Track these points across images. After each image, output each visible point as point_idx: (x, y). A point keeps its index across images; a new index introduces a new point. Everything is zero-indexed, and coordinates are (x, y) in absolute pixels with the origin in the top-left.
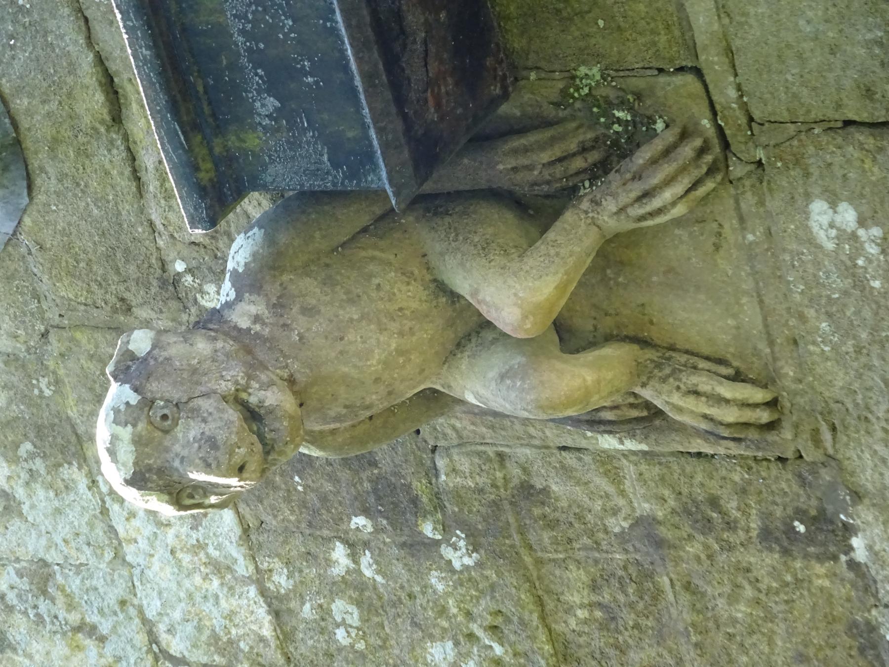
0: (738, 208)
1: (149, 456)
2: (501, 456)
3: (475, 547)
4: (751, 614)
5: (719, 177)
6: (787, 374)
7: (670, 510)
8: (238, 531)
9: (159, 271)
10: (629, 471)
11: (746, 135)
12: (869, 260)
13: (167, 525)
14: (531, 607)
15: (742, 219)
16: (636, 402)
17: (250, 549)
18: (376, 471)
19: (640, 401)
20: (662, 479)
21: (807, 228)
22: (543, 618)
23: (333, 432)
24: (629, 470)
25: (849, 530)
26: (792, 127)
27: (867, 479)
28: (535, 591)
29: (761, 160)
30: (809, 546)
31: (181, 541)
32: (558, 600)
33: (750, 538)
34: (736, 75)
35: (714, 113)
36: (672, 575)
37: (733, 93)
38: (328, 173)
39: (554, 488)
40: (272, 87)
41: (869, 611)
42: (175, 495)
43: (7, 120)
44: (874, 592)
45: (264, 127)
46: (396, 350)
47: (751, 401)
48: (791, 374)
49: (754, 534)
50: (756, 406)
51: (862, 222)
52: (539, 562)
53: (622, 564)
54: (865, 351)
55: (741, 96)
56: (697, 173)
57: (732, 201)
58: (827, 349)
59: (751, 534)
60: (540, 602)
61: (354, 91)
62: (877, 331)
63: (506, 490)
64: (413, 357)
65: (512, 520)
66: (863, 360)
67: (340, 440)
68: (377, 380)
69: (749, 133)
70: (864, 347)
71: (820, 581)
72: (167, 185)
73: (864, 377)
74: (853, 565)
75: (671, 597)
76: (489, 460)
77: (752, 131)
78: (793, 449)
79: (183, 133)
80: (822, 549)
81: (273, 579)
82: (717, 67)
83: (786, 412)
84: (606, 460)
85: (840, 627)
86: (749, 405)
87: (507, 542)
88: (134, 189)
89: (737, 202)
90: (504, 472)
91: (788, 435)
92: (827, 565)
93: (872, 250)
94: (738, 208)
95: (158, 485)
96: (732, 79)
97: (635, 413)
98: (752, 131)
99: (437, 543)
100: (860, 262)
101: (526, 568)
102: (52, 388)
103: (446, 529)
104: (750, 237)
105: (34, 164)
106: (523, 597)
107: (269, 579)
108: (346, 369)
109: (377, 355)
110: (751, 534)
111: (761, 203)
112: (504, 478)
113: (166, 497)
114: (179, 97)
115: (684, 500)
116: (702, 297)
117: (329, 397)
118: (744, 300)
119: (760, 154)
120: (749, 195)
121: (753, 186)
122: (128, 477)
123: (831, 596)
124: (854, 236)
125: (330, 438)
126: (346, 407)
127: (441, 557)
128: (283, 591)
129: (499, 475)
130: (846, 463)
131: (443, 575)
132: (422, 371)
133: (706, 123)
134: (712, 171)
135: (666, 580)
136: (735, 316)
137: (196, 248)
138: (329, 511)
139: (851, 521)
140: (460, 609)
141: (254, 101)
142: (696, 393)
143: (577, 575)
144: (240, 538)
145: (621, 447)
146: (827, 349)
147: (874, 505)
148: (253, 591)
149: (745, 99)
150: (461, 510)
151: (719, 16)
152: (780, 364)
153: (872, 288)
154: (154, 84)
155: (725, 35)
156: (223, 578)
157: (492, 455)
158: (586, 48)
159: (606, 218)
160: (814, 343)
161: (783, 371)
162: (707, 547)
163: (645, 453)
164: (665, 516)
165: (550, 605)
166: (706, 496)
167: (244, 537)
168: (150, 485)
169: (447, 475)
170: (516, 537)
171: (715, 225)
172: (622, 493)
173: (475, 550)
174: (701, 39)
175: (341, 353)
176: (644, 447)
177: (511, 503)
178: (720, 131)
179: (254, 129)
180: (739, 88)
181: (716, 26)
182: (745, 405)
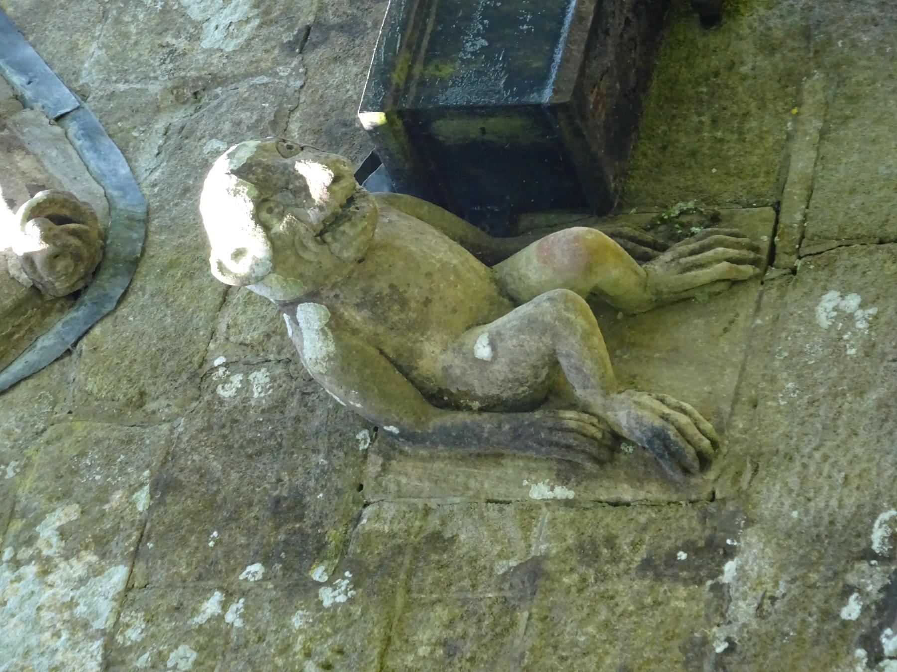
0: (759, 302)
1: (264, 157)
2: (427, 511)
3: (356, 584)
4: (594, 637)
5: (758, 271)
6: (737, 426)
7: (565, 547)
8: (121, 587)
9: (196, 366)
10: (544, 518)
11: (794, 247)
12: (854, 334)
13: (50, 586)
14: (378, 643)
15: (758, 309)
16: (598, 425)
17: (120, 606)
18: (297, 525)
19: (601, 426)
20: (572, 522)
21: (812, 311)
22: (382, 655)
23: (355, 331)
24: (546, 515)
25: (729, 553)
26: (835, 243)
27: (766, 509)
28: (388, 631)
29: (796, 267)
30: (682, 571)
31: (54, 599)
32: (407, 641)
33: (630, 569)
34: (807, 207)
35: (775, 234)
36: (534, 610)
37: (799, 217)
38: (498, 92)
39: (463, 537)
40: (487, 34)
41: (711, 627)
42: (262, 197)
43: (140, 245)
44: (723, 610)
45: (463, 61)
46: (455, 266)
47: (701, 426)
48: (741, 425)
49: (634, 566)
50: (704, 433)
51: (862, 306)
52: (408, 606)
53: (489, 602)
54: (816, 404)
55: (804, 221)
56: (745, 253)
57: (757, 295)
58: (782, 403)
59: (631, 566)
60: (388, 640)
61: (557, 36)
62: (835, 387)
63: (415, 537)
64: (459, 286)
65: (407, 562)
66: (812, 410)
67: (355, 342)
68: (429, 275)
69: (797, 246)
70: (818, 400)
71: (677, 603)
72: (365, 73)
73: (807, 424)
74: (718, 588)
75: (521, 630)
76: (417, 511)
77: (800, 247)
78: (709, 490)
79: (401, 43)
80: (693, 574)
81: (125, 633)
82: (796, 197)
83: (720, 457)
84: (529, 510)
85: (675, 643)
86: (699, 429)
87: (390, 581)
88: (218, 302)
89: (761, 296)
90: (422, 523)
91: (711, 475)
92: (691, 588)
93: (861, 325)
94: (759, 302)
95: (257, 179)
96: (804, 207)
97: (592, 430)
98: (800, 247)
99: (319, 585)
100: (846, 337)
101: (393, 607)
102: (18, 470)
103: (336, 573)
104: (759, 321)
105: (138, 283)
106: (376, 631)
107: (122, 632)
108: (413, 248)
109: (441, 255)
110: (631, 566)
111: (782, 297)
112: (420, 527)
113: (255, 192)
114: (411, 22)
115: (584, 537)
116: (692, 369)
117: (386, 266)
118: (728, 371)
119: (799, 263)
120: (774, 291)
121: (781, 285)
122: (235, 168)
123: (681, 615)
124: (851, 317)
125: (348, 334)
126: (392, 286)
127: (317, 596)
128: (129, 643)
129: (417, 523)
130: (755, 495)
131: (308, 613)
132: (455, 311)
133: (765, 238)
134: (755, 263)
135: (526, 614)
136: (713, 383)
137: (244, 348)
138: (228, 562)
139: (735, 543)
140: (304, 648)
141: (467, 42)
142: (662, 401)
143: (441, 613)
144: (119, 593)
145: (549, 495)
146: (782, 403)
147: (763, 528)
148: (96, 646)
149: (805, 225)
150: (363, 552)
151: (815, 165)
152: (734, 418)
153: (847, 356)
154: (401, 6)
155: (813, 178)
156: (72, 634)
157: (420, 506)
158: (694, 185)
159: (656, 267)
160: (775, 399)
161: (734, 423)
162: (584, 580)
163: (568, 503)
164: (558, 553)
165: (397, 643)
166: (606, 534)
167: (122, 594)
168: (250, 176)
169: (369, 519)
170: (402, 576)
171: (731, 315)
172: (526, 538)
173: (354, 589)
174: (793, 176)
175: (417, 239)
176: (571, 494)
177: (415, 548)
178: (773, 246)
179: (453, 61)
180: (805, 215)
181: (810, 170)
182: (696, 424)
